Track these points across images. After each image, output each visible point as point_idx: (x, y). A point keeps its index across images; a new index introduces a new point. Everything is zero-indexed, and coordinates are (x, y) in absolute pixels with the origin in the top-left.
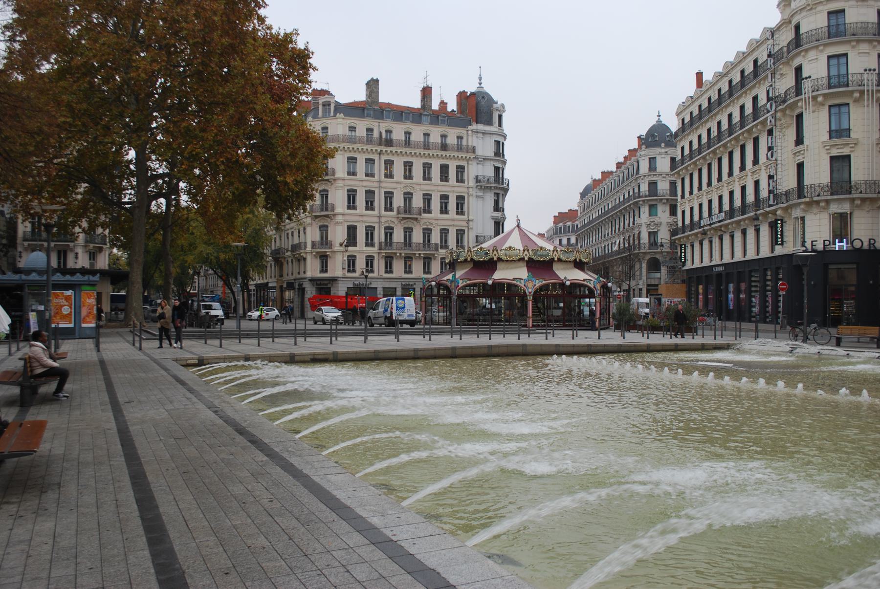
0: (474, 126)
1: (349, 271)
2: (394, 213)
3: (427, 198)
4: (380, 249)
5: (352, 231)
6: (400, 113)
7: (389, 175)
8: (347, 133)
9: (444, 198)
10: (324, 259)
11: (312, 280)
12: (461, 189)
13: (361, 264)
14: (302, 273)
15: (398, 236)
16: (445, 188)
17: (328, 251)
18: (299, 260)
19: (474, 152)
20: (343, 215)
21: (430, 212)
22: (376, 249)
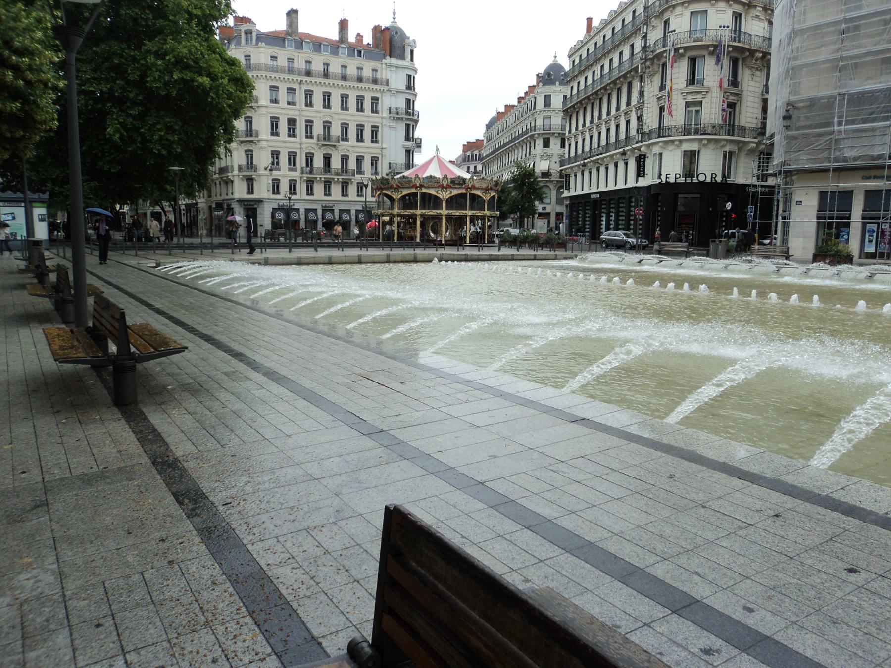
0: (388, 60)
1: (274, 193)
2: (315, 140)
3: (345, 128)
4: (302, 173)
5: (275, 155)
6: (318, 44)
7: (309, 104)
8: (270, 62)
9: (360, 128)
10: (250, 181)
11: (240, 201)
12: (375, 119)
13: (284, 187)
14: (230, 193)
15: (318, 162)
16: (360, 118)
17: (254, 175)
18: (226, 183)
19: (387, 85)
20: (267, 140)
21: (347, 140)
22: (298, 173)
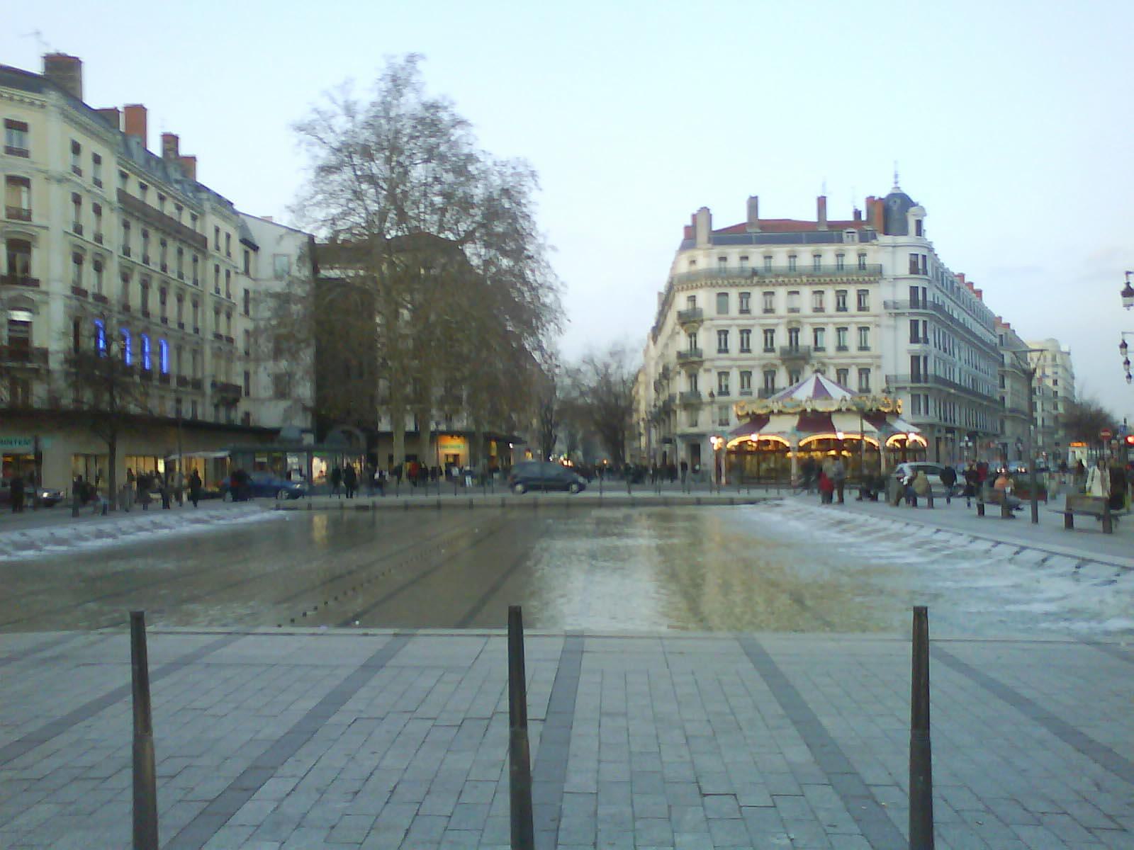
11: (684, 437)
12: (864, 319)
